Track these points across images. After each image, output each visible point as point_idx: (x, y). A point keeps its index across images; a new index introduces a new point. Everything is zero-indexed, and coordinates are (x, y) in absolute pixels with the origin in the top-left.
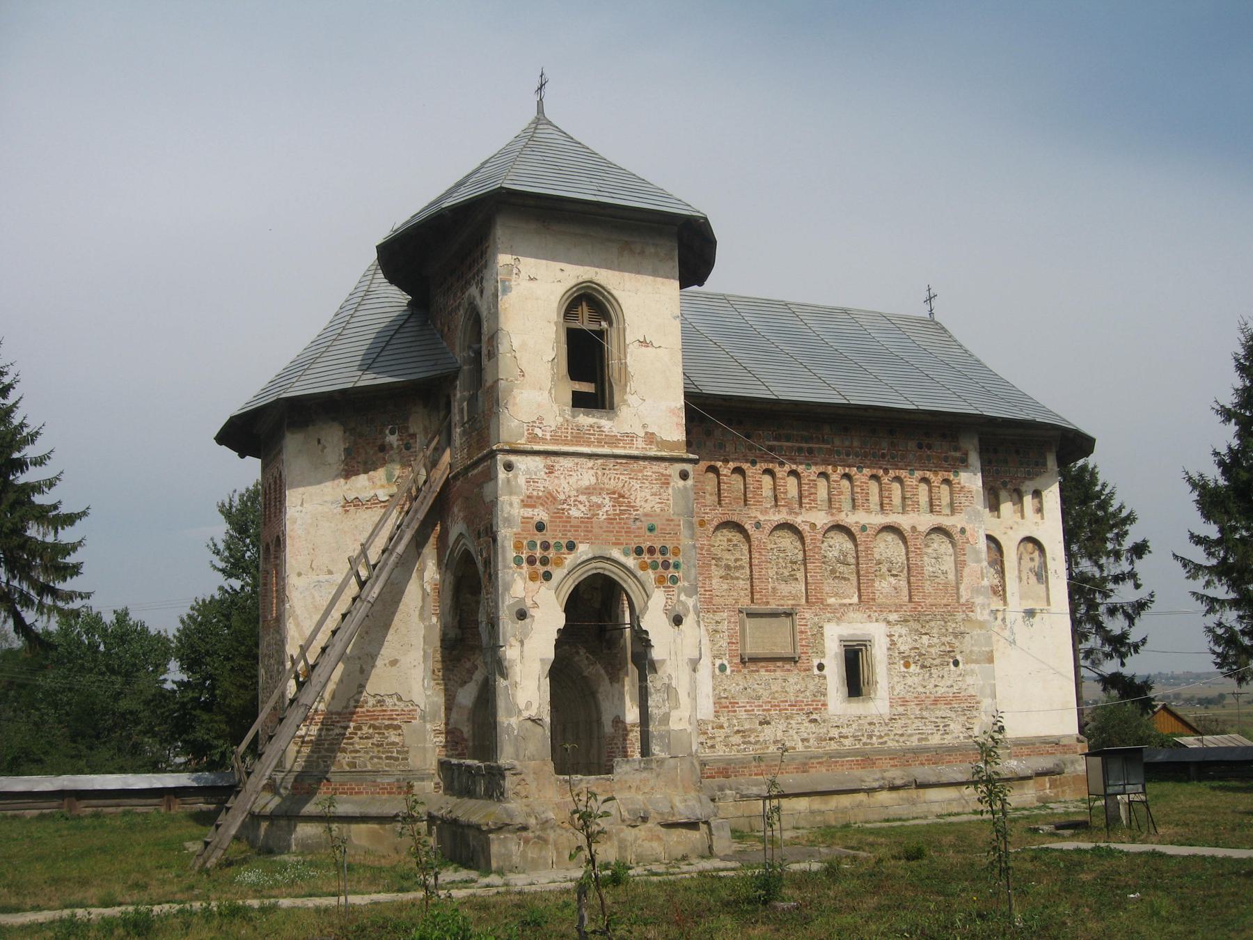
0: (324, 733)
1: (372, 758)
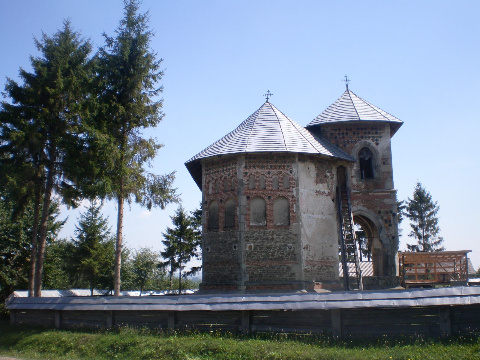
0: (313, 268)
1: (326, 276)
